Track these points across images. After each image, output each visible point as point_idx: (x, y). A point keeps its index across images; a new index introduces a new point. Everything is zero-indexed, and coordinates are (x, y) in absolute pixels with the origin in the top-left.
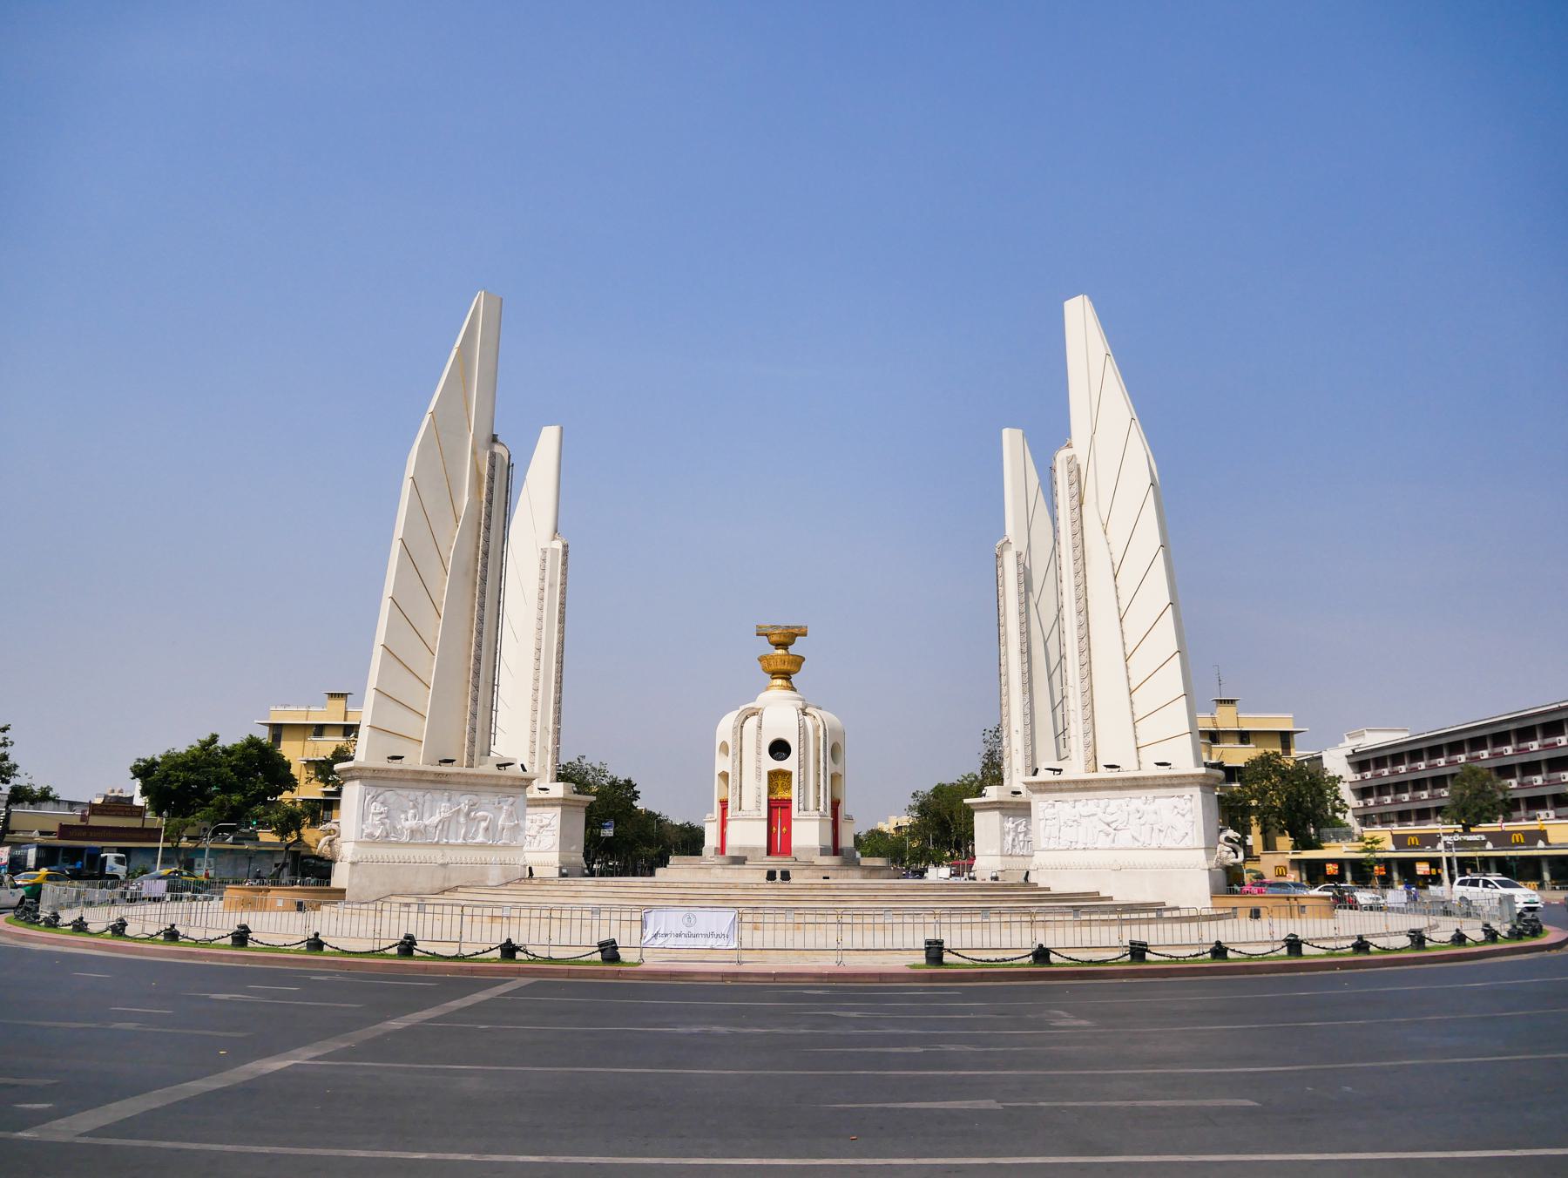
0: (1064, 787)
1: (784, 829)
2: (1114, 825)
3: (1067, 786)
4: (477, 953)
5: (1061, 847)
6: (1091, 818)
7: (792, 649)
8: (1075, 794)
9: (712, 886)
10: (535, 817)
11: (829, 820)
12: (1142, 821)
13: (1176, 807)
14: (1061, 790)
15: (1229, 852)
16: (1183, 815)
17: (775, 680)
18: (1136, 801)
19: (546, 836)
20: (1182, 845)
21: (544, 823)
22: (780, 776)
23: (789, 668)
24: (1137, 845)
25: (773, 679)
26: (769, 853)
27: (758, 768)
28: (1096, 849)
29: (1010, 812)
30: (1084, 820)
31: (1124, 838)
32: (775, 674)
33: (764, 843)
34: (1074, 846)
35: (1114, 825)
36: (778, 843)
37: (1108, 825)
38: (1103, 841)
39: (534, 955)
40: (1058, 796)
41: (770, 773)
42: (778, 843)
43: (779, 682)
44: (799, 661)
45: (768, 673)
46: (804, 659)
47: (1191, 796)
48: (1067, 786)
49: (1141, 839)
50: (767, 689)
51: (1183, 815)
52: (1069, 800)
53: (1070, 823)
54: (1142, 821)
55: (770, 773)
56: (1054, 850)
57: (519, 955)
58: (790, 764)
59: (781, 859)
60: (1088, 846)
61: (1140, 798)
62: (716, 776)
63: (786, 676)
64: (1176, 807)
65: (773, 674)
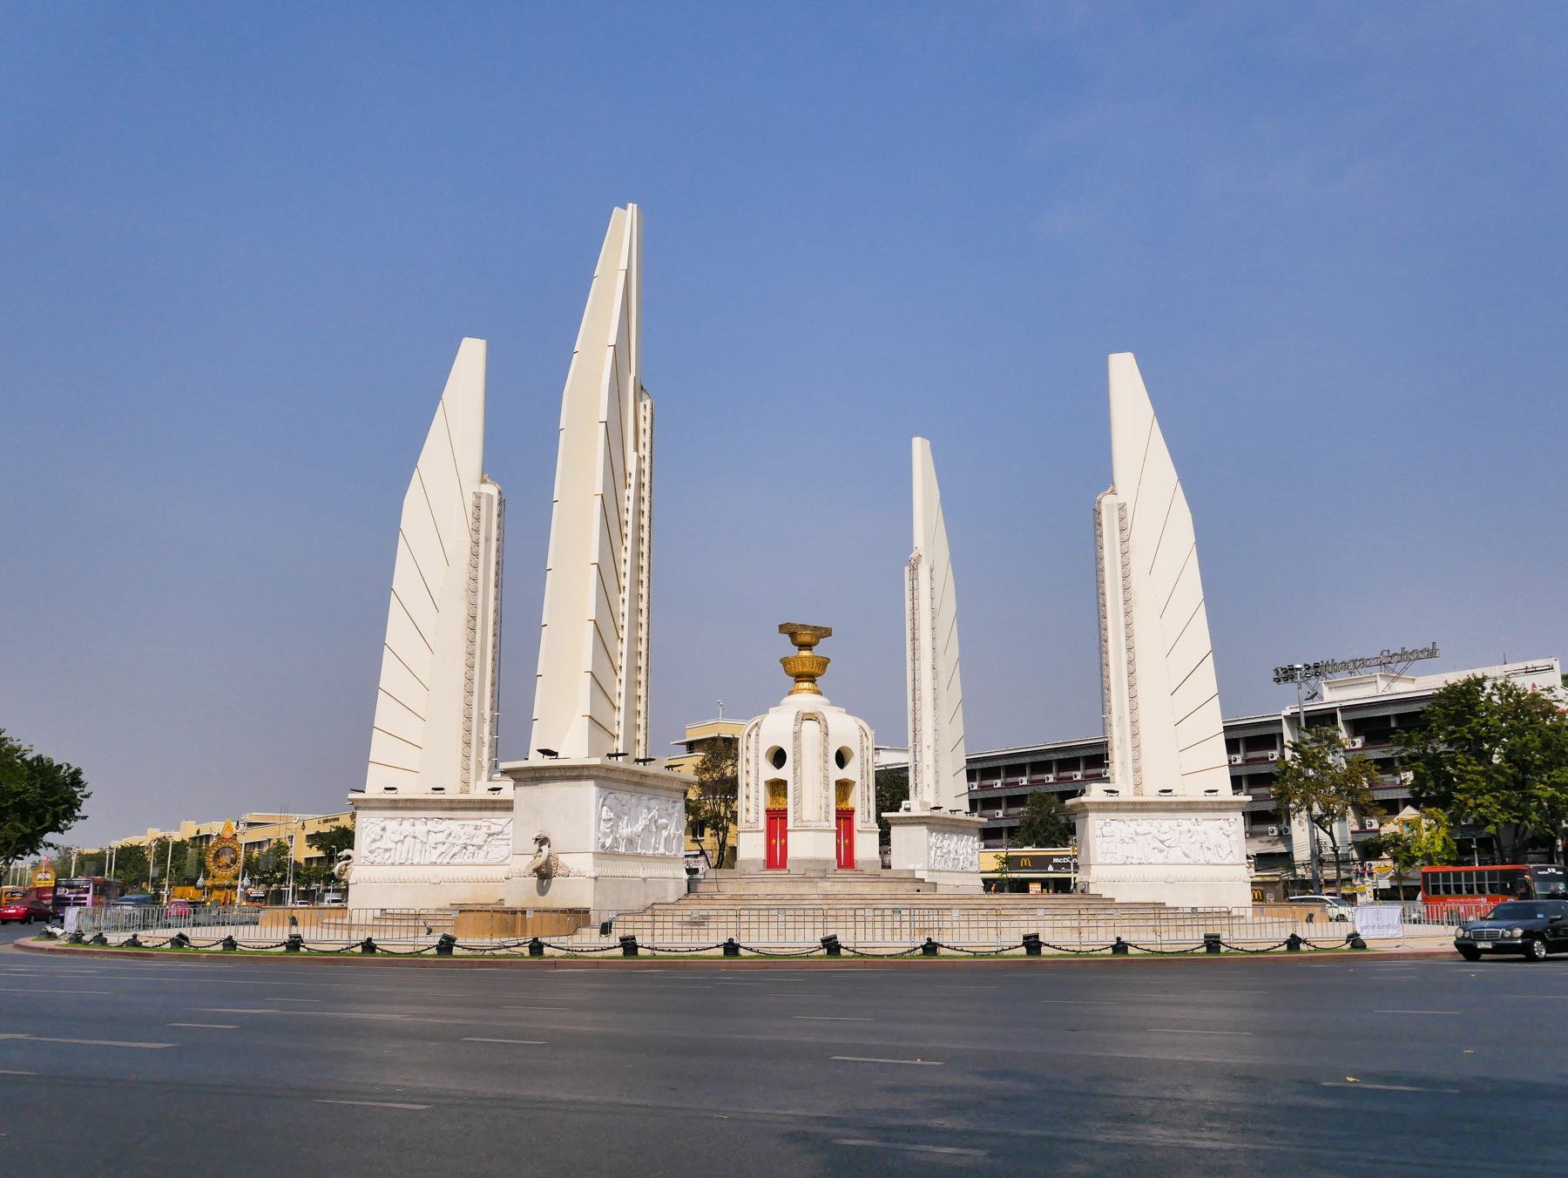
0: (1130, 807)
1: (847, 841)
2: (1167, 843)
3: (1125, 807)
4: (1275, 947)
5: (1117, 862)
6: (1147, 836)
7: (818, 650)
8: (1131, 814)
9: (951, 897)
10: (479, 823)
11: (875, 832)
12: (1193, 840)
13: (1221, 829)
14: (1117, 810)
16: (1228, 836)
17: (801, 684)
18: (1186, 821)
19: (497, 846)
20: (1226, 862)
21: (492, 831)
23: (810, 670)
24: (1186, 860)
25: (797, 682)
26: (840, 866)
27: (826, 777)
28: (1151, 863)
29: (937, 827)
30: (1138, 838)
31: (1175, 855)
32: (799, 677)
33: (831, 854)
34: (1130, 861)
35: (1167, 843)
36: (846, 859)
37: (1161, 842)
38: (1160, 858)
39: (1315, 946)
40: (1114, 815)
42: (846, 859)
43: (806, 685)
44: (824, 663)
45: (791, 675)
46: (829, 660)
47: (1236, 819)
48: (1125, 807)
49: (1191, 855)
50: (791, 693)
51: (1228, 836)
52: (1125, 819)
53: (1127, 840)
54: (1193, 840)
56: (1111, 864)
57: (1303, 947)
58: (851, 772)
59: (844, 872)
60: (1144, 861)
61: (1190, 819)
62: (762, 787)
63: (811, 678)
64: (1221, 829)
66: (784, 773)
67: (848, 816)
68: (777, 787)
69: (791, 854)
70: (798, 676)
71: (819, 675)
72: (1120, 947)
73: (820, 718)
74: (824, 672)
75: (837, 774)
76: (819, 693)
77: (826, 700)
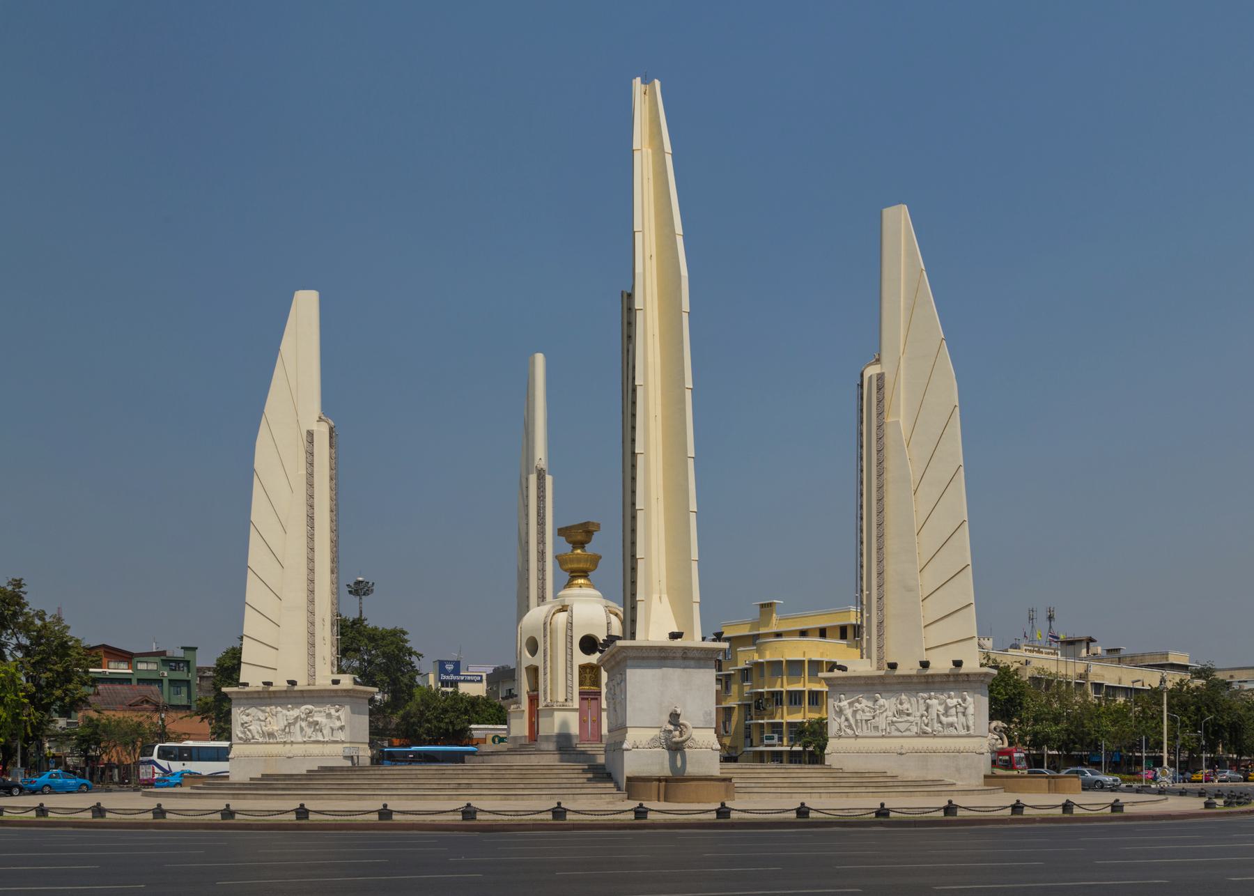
7: (591, 548)
15: (997, 740)
22: (588, 670)
41: (580, 666)
43: (581, 581)
44: (595, 560)
55: (583, 668)
63: (584, 574)
65: (572, 572)
66: (537, 660)
67: (596, 697)
68: (533, 671)
69: (540, 734)
70: (572, 572)
71: (591, 571)
72: (803, 811)
73: (569, 608)
74: (596, 567)
75: (581, 658)
76: (587, 586)
77: (600, 594)
